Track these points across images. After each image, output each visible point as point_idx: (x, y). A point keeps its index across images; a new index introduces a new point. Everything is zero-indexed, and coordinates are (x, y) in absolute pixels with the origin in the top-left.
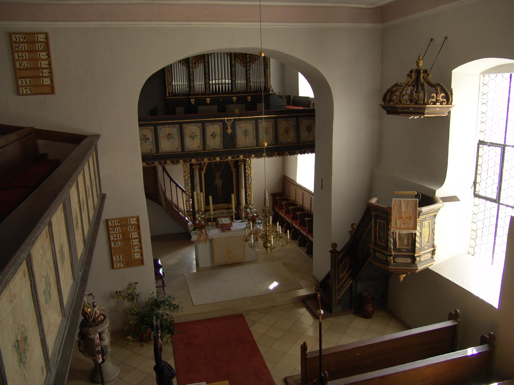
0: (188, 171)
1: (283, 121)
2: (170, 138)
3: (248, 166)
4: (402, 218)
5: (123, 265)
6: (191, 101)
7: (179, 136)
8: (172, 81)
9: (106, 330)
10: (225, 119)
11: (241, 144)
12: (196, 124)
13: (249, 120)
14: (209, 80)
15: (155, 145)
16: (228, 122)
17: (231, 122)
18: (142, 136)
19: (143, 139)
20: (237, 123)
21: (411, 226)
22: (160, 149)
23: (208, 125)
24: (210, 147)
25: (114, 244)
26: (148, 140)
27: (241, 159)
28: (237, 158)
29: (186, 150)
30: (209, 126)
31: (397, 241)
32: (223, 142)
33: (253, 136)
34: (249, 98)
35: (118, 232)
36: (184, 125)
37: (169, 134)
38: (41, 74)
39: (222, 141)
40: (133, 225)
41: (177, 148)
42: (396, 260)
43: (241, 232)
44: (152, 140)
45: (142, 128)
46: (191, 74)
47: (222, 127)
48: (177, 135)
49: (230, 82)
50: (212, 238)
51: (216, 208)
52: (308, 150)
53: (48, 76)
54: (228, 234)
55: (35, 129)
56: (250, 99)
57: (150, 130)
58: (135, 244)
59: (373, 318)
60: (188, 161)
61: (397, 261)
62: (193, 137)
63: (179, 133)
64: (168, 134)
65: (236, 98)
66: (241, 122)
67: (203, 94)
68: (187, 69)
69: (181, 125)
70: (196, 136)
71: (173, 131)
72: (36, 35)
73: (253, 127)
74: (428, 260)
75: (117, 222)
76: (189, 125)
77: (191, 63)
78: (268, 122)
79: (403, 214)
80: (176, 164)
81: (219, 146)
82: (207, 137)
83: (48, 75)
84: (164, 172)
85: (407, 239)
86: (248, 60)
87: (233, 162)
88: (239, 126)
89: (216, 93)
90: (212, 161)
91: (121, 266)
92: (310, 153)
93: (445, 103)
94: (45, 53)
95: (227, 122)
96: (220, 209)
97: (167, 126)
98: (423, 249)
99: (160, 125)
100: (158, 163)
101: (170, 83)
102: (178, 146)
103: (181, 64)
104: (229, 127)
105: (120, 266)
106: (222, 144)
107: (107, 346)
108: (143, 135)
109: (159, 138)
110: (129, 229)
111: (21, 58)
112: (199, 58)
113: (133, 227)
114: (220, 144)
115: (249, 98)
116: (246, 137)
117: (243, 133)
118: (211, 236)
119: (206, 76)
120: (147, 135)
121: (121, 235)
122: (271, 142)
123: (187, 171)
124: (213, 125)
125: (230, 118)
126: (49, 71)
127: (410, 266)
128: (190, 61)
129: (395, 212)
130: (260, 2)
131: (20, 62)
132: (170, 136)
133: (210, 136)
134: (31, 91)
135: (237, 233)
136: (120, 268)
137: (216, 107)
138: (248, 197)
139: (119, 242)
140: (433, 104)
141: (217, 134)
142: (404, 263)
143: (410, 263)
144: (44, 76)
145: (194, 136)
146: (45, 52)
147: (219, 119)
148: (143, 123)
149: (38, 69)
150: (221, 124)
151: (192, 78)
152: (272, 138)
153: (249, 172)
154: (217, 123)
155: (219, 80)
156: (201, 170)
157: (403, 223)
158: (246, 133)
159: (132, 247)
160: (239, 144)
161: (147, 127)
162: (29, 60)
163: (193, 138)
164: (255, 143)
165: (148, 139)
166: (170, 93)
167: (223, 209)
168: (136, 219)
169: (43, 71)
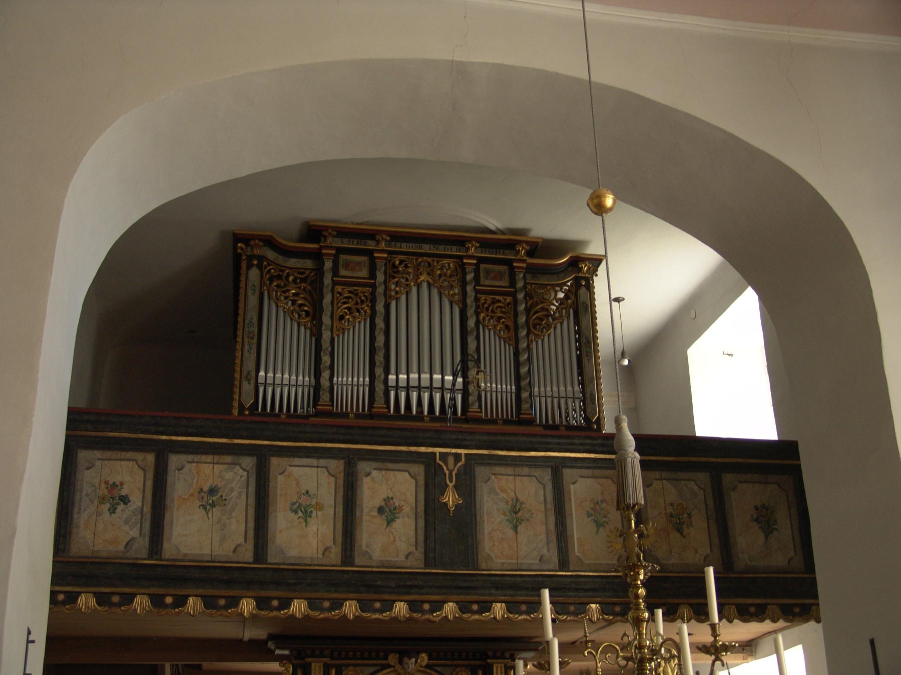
2: (213, 505)
7: (252, 501)
8: (258, 371)
10: (435, 453)
11: (496, 558)
12: (323, 462)
13: (530, 466)
14: (387, 372)
16: (447, 466)
17: (459, 465)
18: (103, 486)
19: (103, 499)
20: (481, 472)
22: (166, 545)
23: (368, 470)
24: (371, 557)
26: (125, 504)
27: (499, 617)
29: (273, 558)
30: (372, 475)
32: (425, 541)
33: (543, 529)
36: (275, 461)
37: (212, 491)
39: (421, 538)
41: (236, 548)
44: (140, 504)
46: (323, 348)
47: (422, 481)
48: (244, 497)
57: (139, 466)
60: (275, 603)
63: (252, 489)
64: (206, 489)
66: (498, 469)
68: (314, 339)
69: (262, 457)
70: (319, 507)
71: (227, 477)
73: (545, 494)
77: (329, 314)
78: (600, 480)
80: (225, 613)
81: (407, 557)
86: (522, 319)
88: (489, 483)
90: (377, 616)
97: (210, 458)
101: (249, 373)
102: (241, 540)
104: (451, 481)
109: (168, 502)
112: (357, 304)
114: (413, 549)
116: (518, 528)
117: (504, 514)
119: (376, 357)
120: (122, 484)
125: (454, 451)
128: (325, 307)
132: (215, 498)
133: (375, 513)
141: (400, 508)
147: (413, 449)
148: (117, 434)
150: (419, 469)
151: (326, 359)
154: (403, 466)
161: (129, 455)
163: (307, 515)
164: (556, 560)
165: (125, 500)
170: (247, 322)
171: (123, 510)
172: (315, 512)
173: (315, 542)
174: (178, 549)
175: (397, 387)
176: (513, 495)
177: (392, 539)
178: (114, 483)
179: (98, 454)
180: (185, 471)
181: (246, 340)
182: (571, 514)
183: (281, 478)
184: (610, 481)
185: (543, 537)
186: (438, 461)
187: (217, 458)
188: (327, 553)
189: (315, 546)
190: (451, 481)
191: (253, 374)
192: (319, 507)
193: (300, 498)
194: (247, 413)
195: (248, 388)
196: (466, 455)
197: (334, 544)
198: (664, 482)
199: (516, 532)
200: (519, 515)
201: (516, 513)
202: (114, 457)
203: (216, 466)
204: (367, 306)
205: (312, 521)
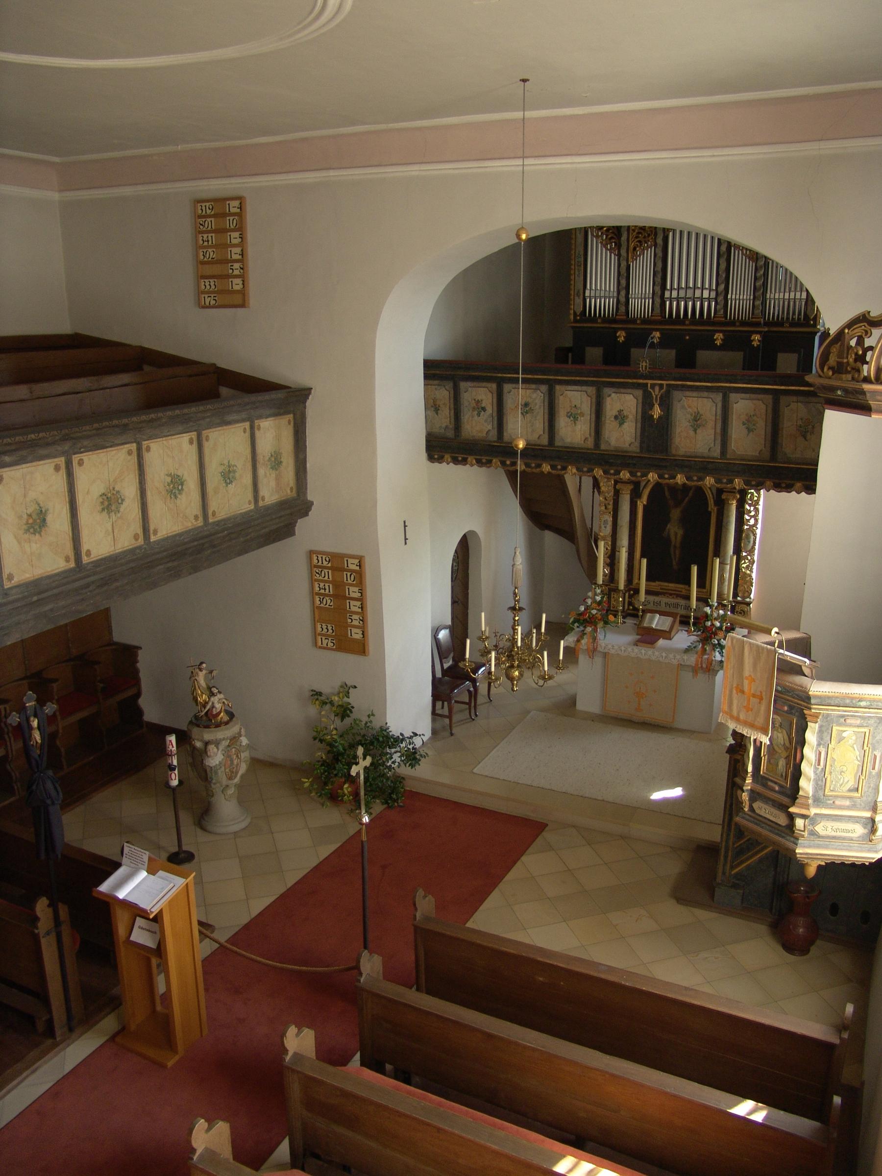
0: (610, 495)
1: (797, 402)
2: (527, 413)
3: (750, 506)
4: (743, 692)
5: (332, 644)
6: (752, 339)
7: (546, 411)
9: (224, 742)
10: (647, 384)
12: (584, 388)
15: (495, 422)
18: (473, 401)
20: (677, 394)
21: (760, 721)
22: (505, 434)
23: (609, 393)
24: (610, 444)
25: (320, 601)
26: (484, 411)
28: (669, 479)
29: (558, 443)
31: (764, 756)
34: (756, 338)
35: (326, 578)
38: (231, 271)
39: (639, 434)
40: (352, 571)
42: (755, 805)
43: (671, 656)
45: (431, 382)
47: (640, 400)
48: (542, 408)
49: (714, 297)
50: (606, 651)
51: (661, 589)
52: (798, 485)
53: (240, 275)
54: (643, 651)
55: (218, 368)
56: (759, 341)
58: (353, 609)
59: (805, 957)
61: (757, 811)
62: (574, 417)
63: (546, 403)
64: (523, 403)
65: (661, 334)
66: (688, 393)
67: (645, 321)
70: (582, 414)
72: (228, 202)
75: (326, 561)
78: (754, 401)
79: (746, 682)
82: (605, 420)
83: (239, 273)
84: (595, 490)
85: (786, 758)
87: (714, 491)
89: (678, 320)
91: (329, 646)
92: (803, 493)
94: (237, 234)
95: (652, 391)
96: (671, 594)
98: (832, 802)
99: (508, 383)
100: (474, 461)
101: (578, 291)
102: (542, 433)
103: (607, 249)
106: (638, 441)
108: (475, 400)
109: (505, 411)
110: (345, 579)
111: (206, 243)
112: (645, 237)
113: (352, 576)
114: (633, 440)
115: (756, 338)
116: (697, 431)
117: (689, 422)
118: (603, 645)
120: (482, 401)
122: (759, 453)
123: (608, 494)
126: (242, 266)
127: (783, 834)
129: (732, 672)
130: (524, 111)
131: (205, 251)
135: (664, 654)
137: (672, 353)
139: (327, 598)
141: (627, 417)
143: (785, 826)
144: (236, 275)
145: (577, 414)
146: (237, 231)
150: (639, 393)
152: (763, 442)
153: (752, 522)
154: (629, 391)
155: (673, 292)
156: (636, 494)
158: (697, 421)
159: (348, 615)
160: (677, 446)
161: (484, 384)
162: (215, 246)
163: (575, 419)
164: (718, 451)
165: (484, 409)
167: (678, 596)
168: (358, 561)
169: (233, 266)
170: (577, 255)
173: (580, 434)
174: (511, 436)
175: (671, 299)
176: (696, 410)
177: (622, 434)
178: (478, 400)
179: (469, 384)
180: (511, 393)
181: (576, 267)
182: (732, 422)
183: (561, 398)
184: (761, 402)
185: (713, 437)
186: (649, 389)
187: (528, 385)
188: (586, 441)
189: (580, 437)
190: (656, 402)
192: (582, 414)
193: (571, 409)
195: (579, 301)
196: (667, 385)
198: (799, 404)
199: (696, 433)
200: (699, 422)
201: (696, 421)
205: (578, 423)
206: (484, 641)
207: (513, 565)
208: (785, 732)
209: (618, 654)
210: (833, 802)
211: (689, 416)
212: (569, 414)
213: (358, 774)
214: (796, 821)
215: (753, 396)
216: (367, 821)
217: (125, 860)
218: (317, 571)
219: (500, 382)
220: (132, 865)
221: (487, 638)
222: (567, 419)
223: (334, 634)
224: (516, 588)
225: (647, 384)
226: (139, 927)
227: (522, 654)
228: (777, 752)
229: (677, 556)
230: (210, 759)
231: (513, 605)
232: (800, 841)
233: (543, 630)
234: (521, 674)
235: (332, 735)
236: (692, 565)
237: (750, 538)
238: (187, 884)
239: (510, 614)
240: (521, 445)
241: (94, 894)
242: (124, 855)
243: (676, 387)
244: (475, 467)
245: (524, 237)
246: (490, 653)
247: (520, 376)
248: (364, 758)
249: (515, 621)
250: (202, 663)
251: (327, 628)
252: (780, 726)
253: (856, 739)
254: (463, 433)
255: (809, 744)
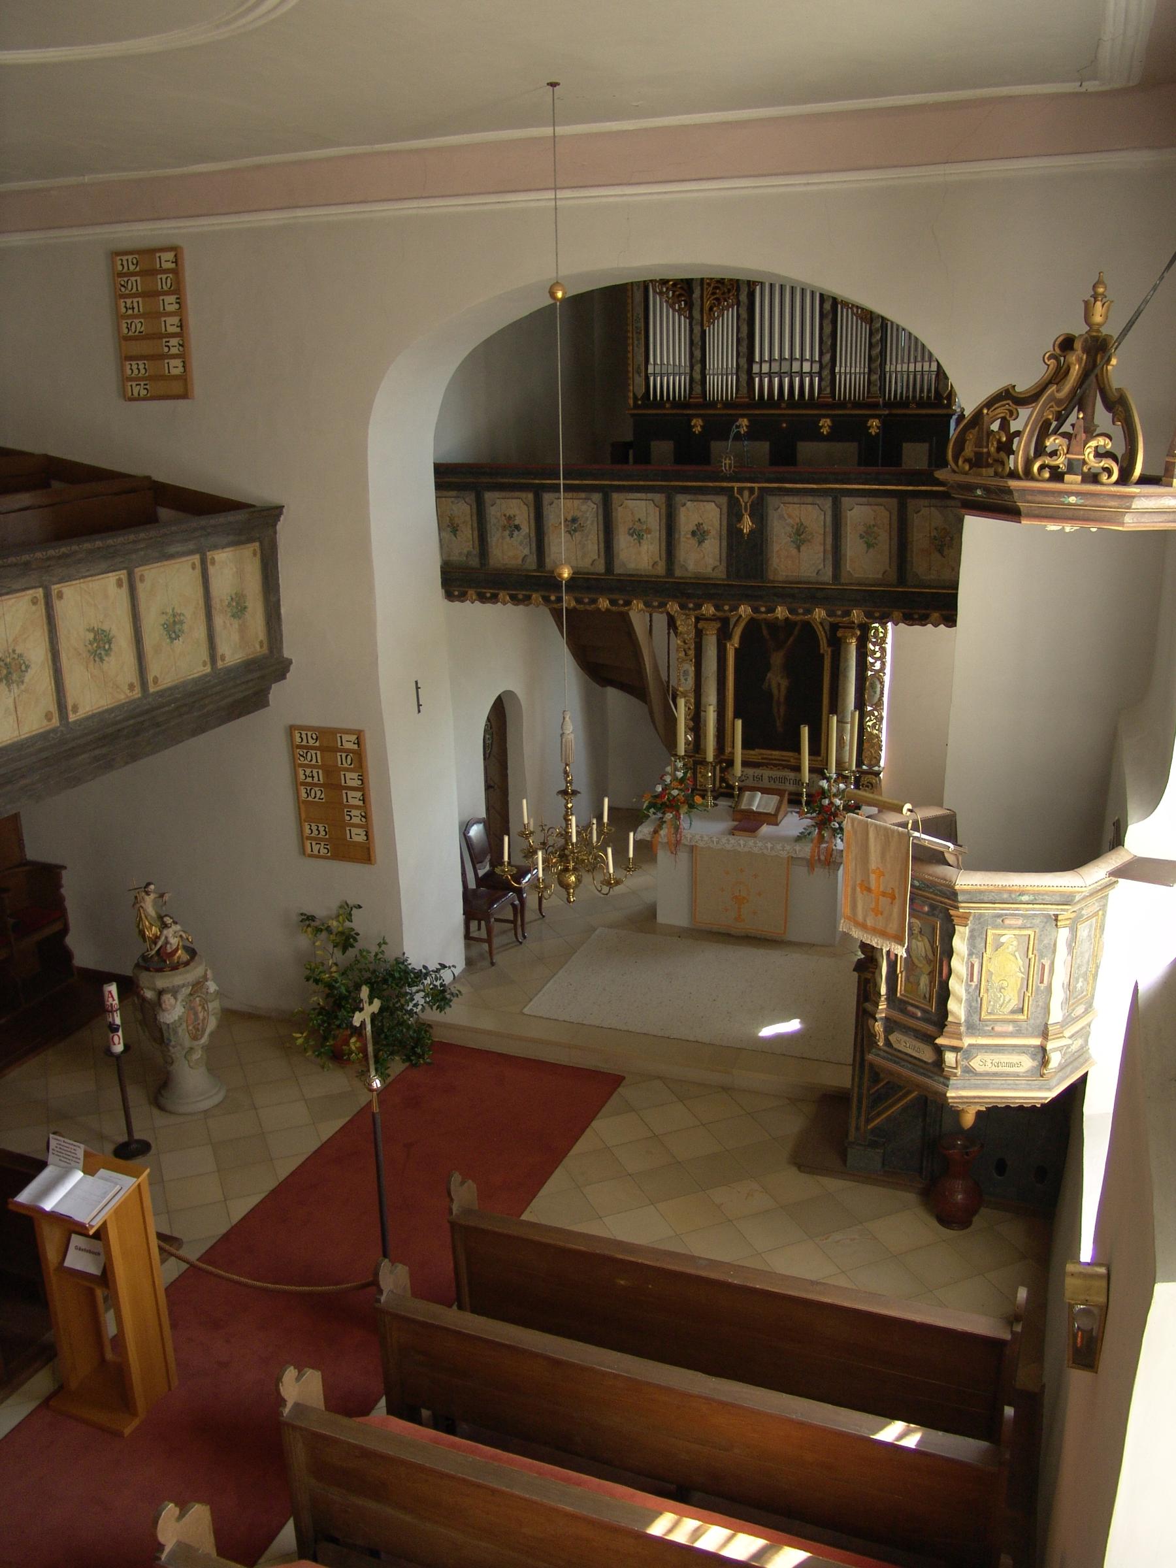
0: (690, 636)
1: (930, 506)
2: (575, 531)
3: (874, 646)
4: (869, 890)
5: (326, 851)
6: (869, 425)
7: (601, 527)
9: (183, 989)
10: (733, 488)
12: (650, 496)
15: (534, 545)
16: (742, 497)
18: (504, 518)
20: (772, 501)
21: (893, 928)
22: (547, 560)
23: (683, 501)
24: (687, 570)
25: (306, 793)
26: (519, 531)
29: (618, 570)
31: (901, 972)
35: (314, 762)
37: (574, 520)
38: (166, 349)
39: (724, 555)
40: (348, 751)
42: (892, 1038)
43: (779, 847)
44: (528, 531)
45: (445, 493)
48: (595, 524)
49: (817, 370)
50: (693, 844)
51: (762, 759)
52: (935, 615)
53: (177, 354)
54: (742, 842)
57: (525, 504)
58: (352, 802)
61: (895, 1046)
62: (637, 534)
63: (601, 517)
64: (569, 518)
66: (787, 499)
67: (727, 405)
70: (649, 531)
72: (158, 255)
74: (1017, 1075)
76: (628, 498)
77: (699, 309)
79: (873, 877)
81: (713, 570)
84: (671, 631)
85: (929, 974)
87: (827, 628)
88: (779, 510)
89: (771, 403)
91: (321, 854)
92: (942, 626)
93: (1110, 476)
94: (171, 299)
95: (739, 496)
96: (775, 765)
98: (990, 1028)
99: (549, 492)
103: (674, 310)
104: (746, 511)
105: (319, 852)
106: (724, 564)
107: (171, 1026)
109: (545, 528)
110: (340, 763)
111: (130, 312)
112: (723, 293)
113: (349, 757)
114: (718, 564)
115: (875, 423)
116: (801, 549)
118: (689, 836)
120: (514, 516)
121: (320, 772)
123: (688, 635)
124: (698, 501)
128: (695, 301)
129: (854, 864)
130: (554, 126)
131: (129, 322)
132: (576, 525)
133: (689, 536)
134: (146, 389)
135: (769, 845)
136: (318, 857)
137: (764, 447)
138: (866, 745)
139: (317, 789)
140: (1051, 479)
142: (911, 1056)
144: (172, 355)
146: (172, 294)
149: (160, 336)
150: (723, 500)
152: (888, 561)
153: (878, 666)
154: (709, 497)
155: (763, 365)
156: (724, 635)
157: (873, 910)
158: (800, 536)
161: (517, 494)
163: (640, 537)
164: (830, 573)
165: (517, 527)
166: (639, 397)
167: (785, 767)
168: (356, 737)
169: (168, 342)
170: (635, 318)
171: (518, 535)
172: (645, 536)
173: (646, 558)
175: (760, 374)
179: (497, 494)
180: (554, 505)
181: (635, 336)
183: (620, 509)
185: (821, 555)
187: (575, 494)
190: (746, 511)
191: (643, 368)
192: (649, 531)
193: (634, 524)
194: (640, 402)
196: (759, 488)
197: (660, 559)
198: (932, 508)
199: (799, 551)
200: (802, 537)
201: (800, 535)
202: (507, 496)
203: (575, 501)
204: (733, 295)
206: (527, 838)
207: (562, 735)
208: (926, 940)
209: (709, 848)
210: (993, 1028)
211: (789, 529)
212: (631, 531)
213: (363, 1023)
214: (946, 1056)
215: (871, 500)
216: (379, 1085)
217: (51, 1158)
218: (302, 753)
219: (538, 491)
220: (63, 1164)
221: (532, 833)
222: (629, 538)
223: (327, 836)
224: (567, 765)
225: (733, 488)
226: (76, 1248)
227: (578, 853)
228: (917, 966)
229: (782, 714)
230: (166, 1014)
231: (564, 788)
232: (951, 1082)
233: (606, 820)
234: (579, 880)
235: (331, 973)
236: (802, 726)
237: (876, 687)
238: (139, 1185)
239: (561, 800)
240: (566, 574)
241: (11, 1207)
242: (51, 1150)
243: (771, 491)
244: (477, 603)
245: (560, 295)
246: (535, 853)
247: (562, 482)
248: (371, 1003)
249: (568, 808)
250: (148, 884)
251: (317, 830)
252: (920, 932)
253: (1018, 945)
254: (490, 561)
255: (957, 954)
